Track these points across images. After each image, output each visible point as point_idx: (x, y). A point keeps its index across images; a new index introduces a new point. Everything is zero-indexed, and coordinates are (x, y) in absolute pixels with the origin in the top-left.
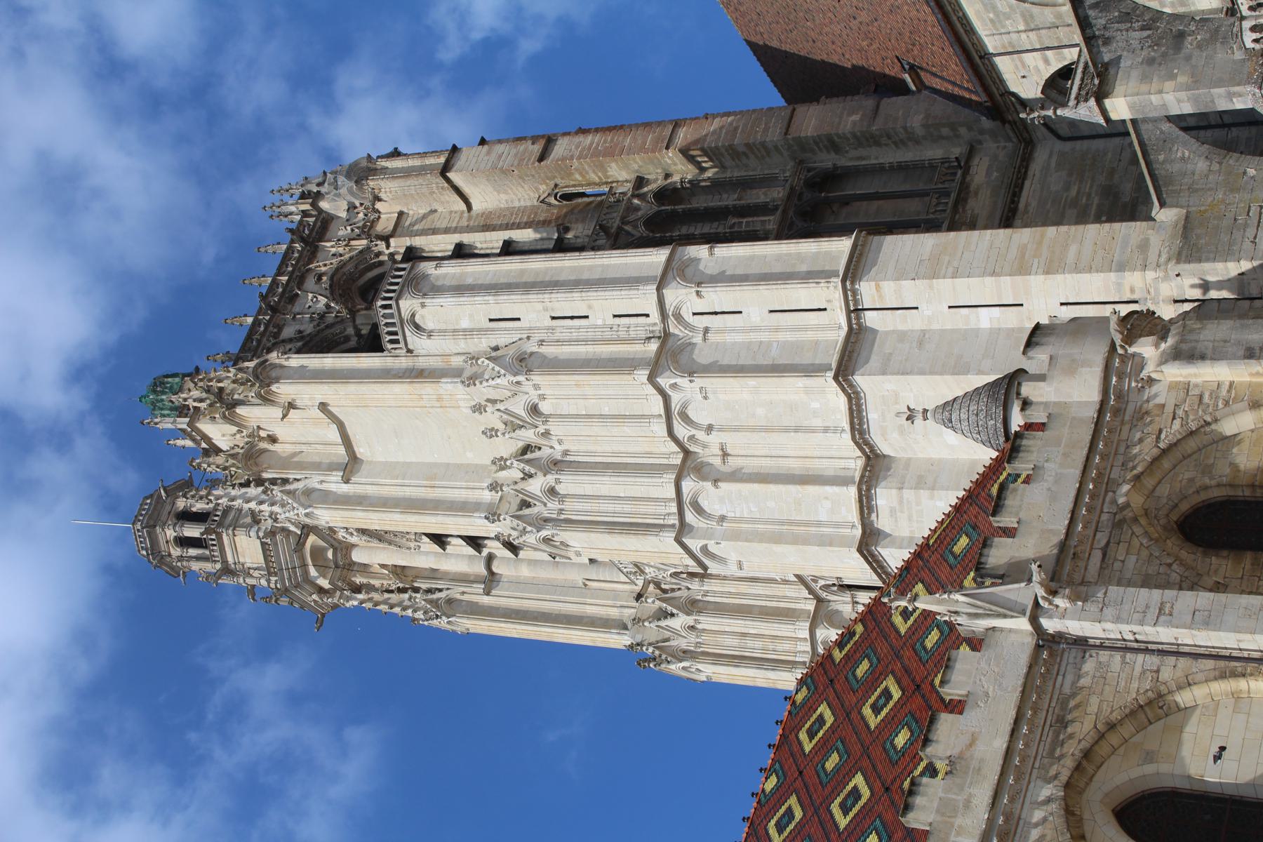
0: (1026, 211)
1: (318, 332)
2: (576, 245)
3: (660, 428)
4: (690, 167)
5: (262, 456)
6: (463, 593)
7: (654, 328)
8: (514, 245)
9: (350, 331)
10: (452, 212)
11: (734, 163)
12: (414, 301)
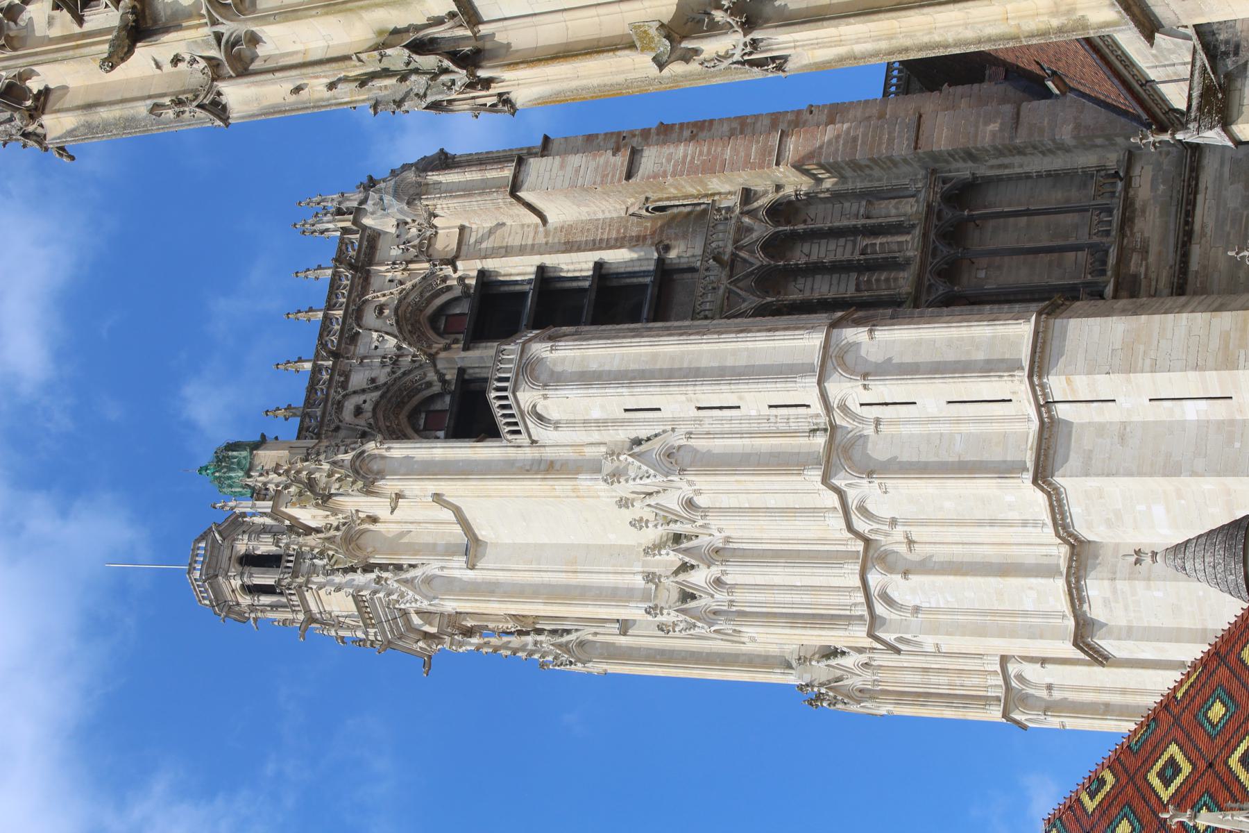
0: (1203, 234)
1: (395, 380)
2: (681, 267)
4: (805, 178)
5: (362, 537)
6: (596, 634)
7: (818, 421)
8: (607, 266)
9: (432, 376)
10: (523, 225)
11: (856, 174)
12: (535, 393)
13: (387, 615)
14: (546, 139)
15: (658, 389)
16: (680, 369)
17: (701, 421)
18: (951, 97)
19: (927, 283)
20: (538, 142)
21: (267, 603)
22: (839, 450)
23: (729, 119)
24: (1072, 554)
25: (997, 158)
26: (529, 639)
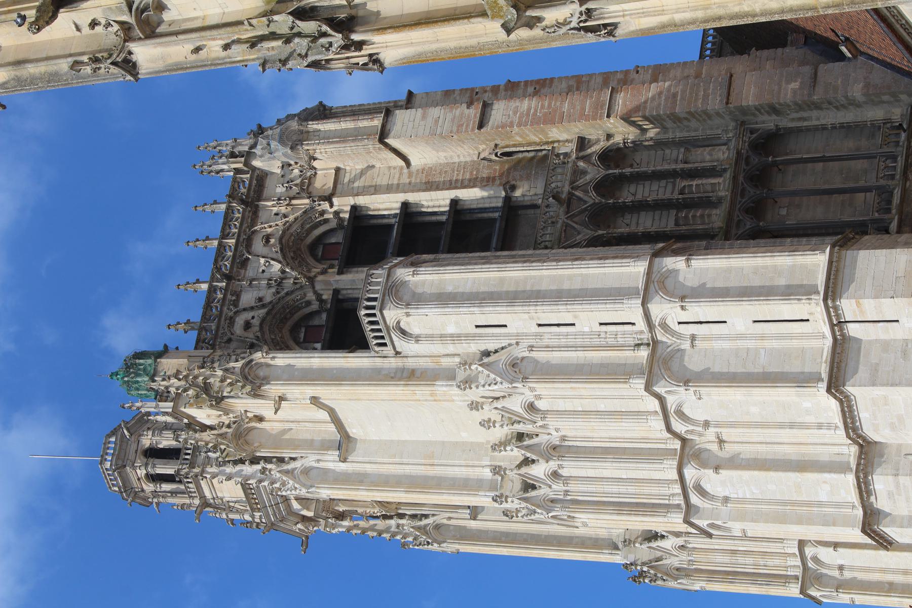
1: (279, 299)
3: (658, 424)
4: (632, 129)
5: (250, 433)
6: (450, 518)
7: (642, 337)
8: (462, 203)
9: (311, 296)
10: (390, 168)
11: (675, 125)
12: (399, 311)
13: (270, 501)
14: (410, 94)
15: (504, 308)
16: (524, 291)
17: (541, 336)
18: (758, 60)
19: (736, 219)
20: (403, 97)
21: (168, 490)
22: (660, 362)
23: (567, 78)
24: (861, 453)
25: (797, 112)
26: (393, 522)
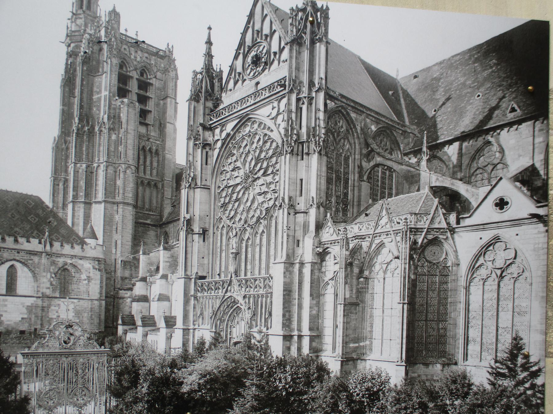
9: (131, 69)
